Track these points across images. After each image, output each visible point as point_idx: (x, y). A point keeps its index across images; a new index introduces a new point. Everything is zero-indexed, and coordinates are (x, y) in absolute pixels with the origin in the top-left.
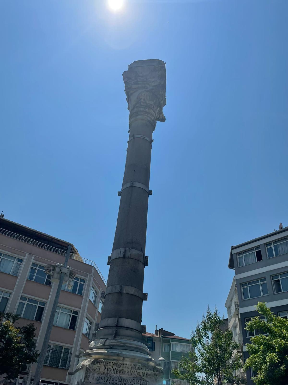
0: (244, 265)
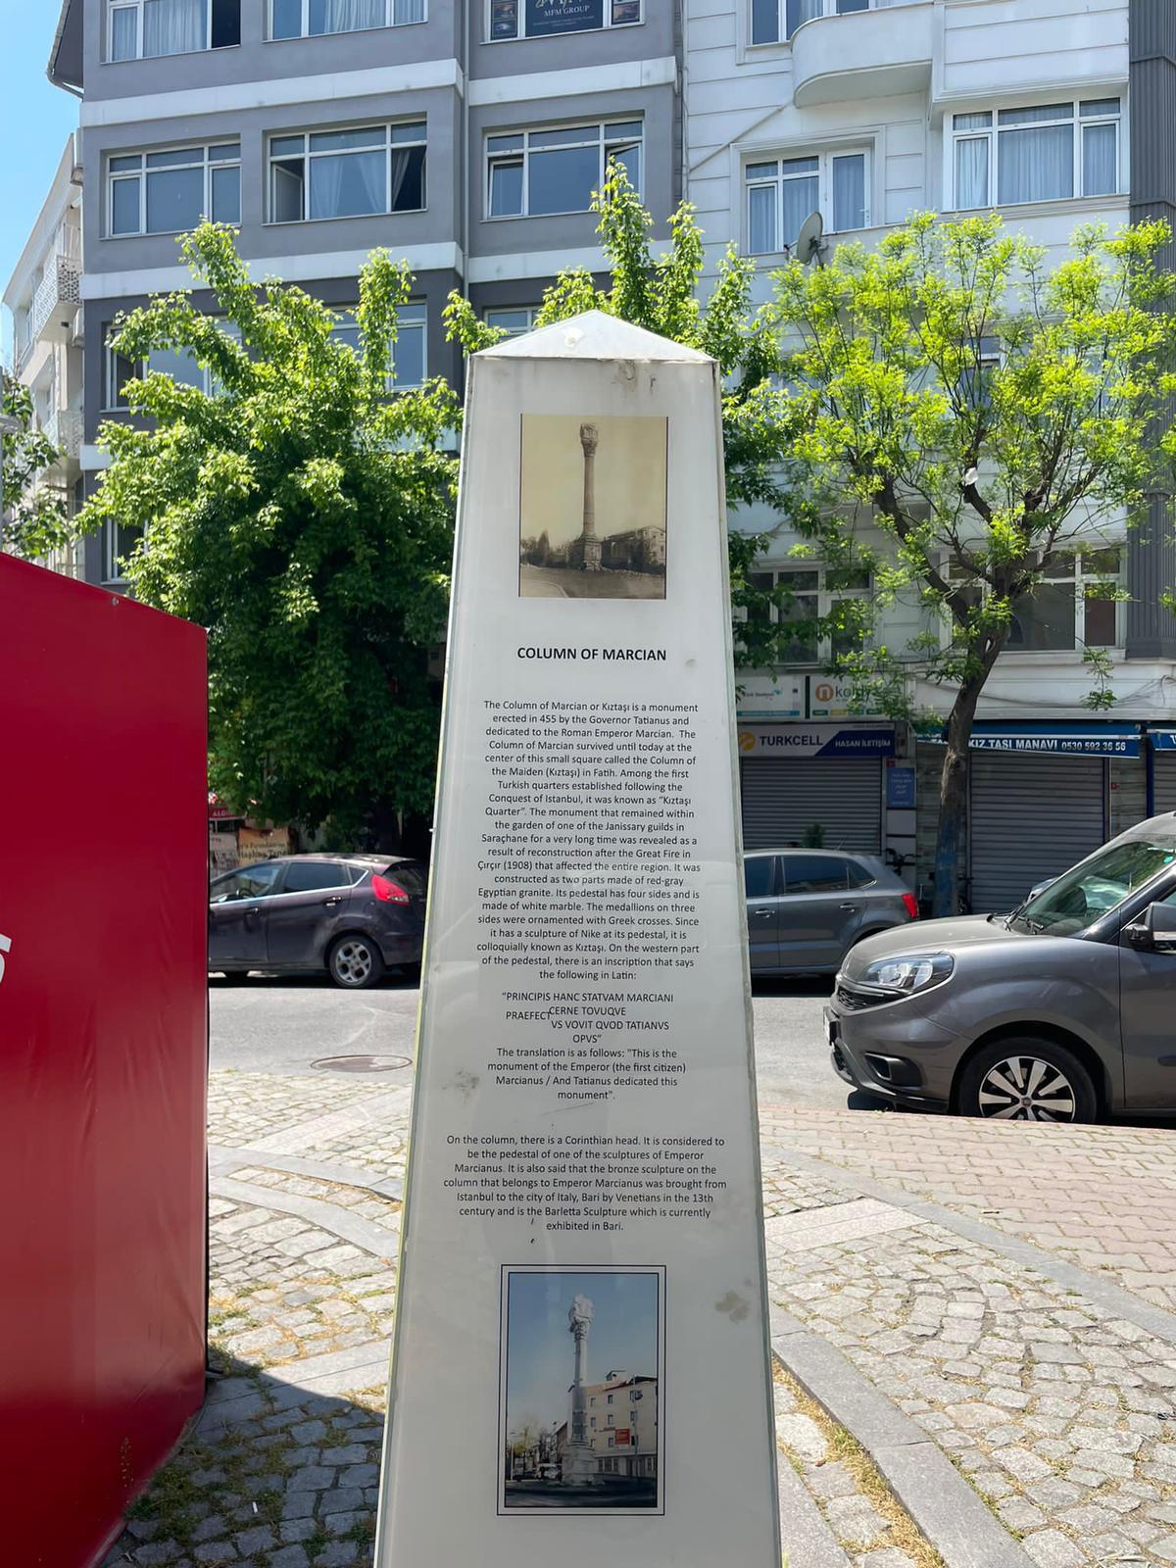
0: (139, 55)
